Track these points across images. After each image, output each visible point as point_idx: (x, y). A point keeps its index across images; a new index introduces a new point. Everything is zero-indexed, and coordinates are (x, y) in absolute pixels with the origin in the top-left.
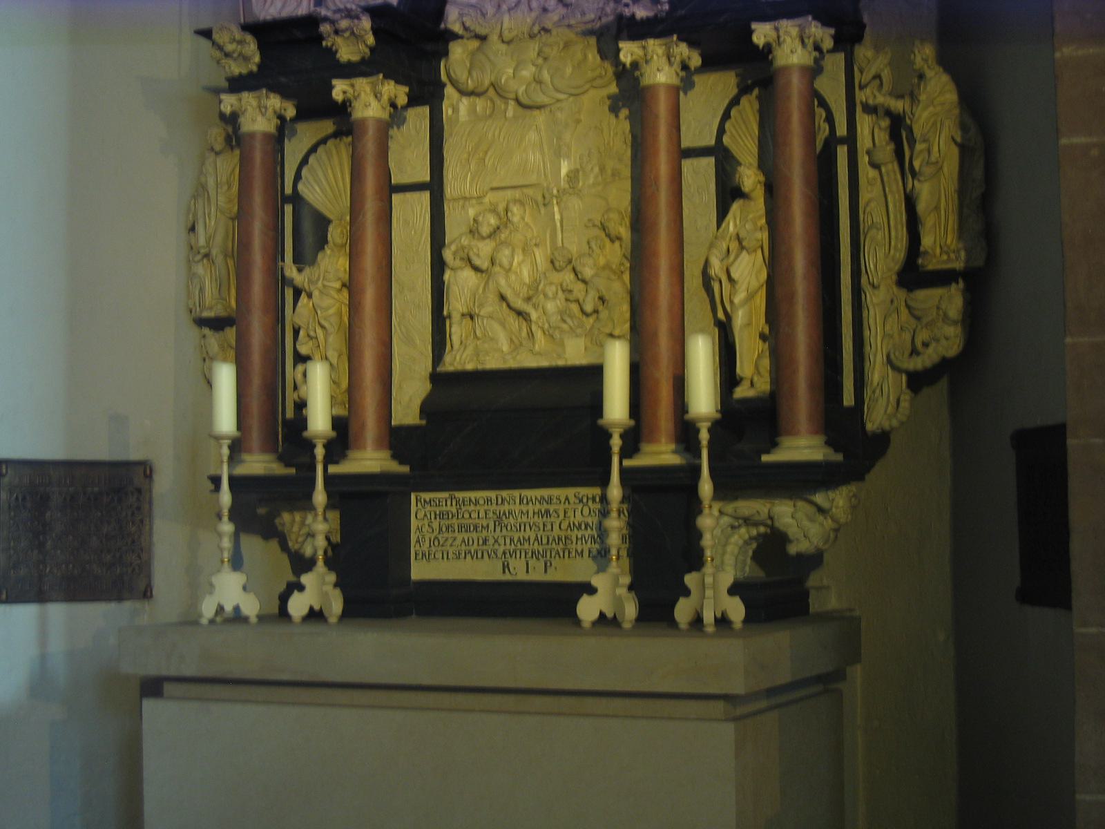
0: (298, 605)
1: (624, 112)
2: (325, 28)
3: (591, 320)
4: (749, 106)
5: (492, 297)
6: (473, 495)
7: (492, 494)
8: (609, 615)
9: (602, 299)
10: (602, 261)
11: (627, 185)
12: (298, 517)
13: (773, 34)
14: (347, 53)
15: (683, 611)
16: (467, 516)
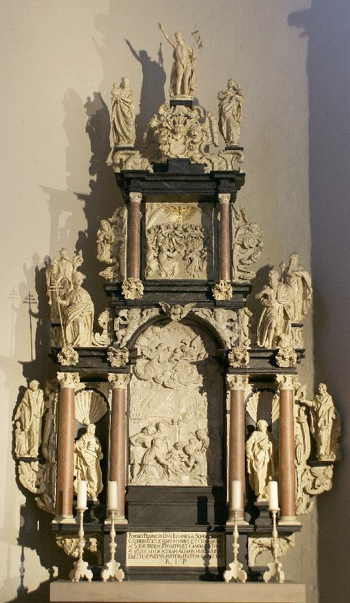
0: (106, 575)
1: (205, 394)
2: (110, 354)
3: (189, 469)
4: (256, 396)
5: (152, 457)
6: (154, 534)
7: (162, 533)
8: (235, 578)
9: (196, 462)
10: (195, 449)
11: (206, 420)
12: (74, 540)
13: (283, 379)
14: (116, 363)
15: (267, 576)
16: (151, 541)
